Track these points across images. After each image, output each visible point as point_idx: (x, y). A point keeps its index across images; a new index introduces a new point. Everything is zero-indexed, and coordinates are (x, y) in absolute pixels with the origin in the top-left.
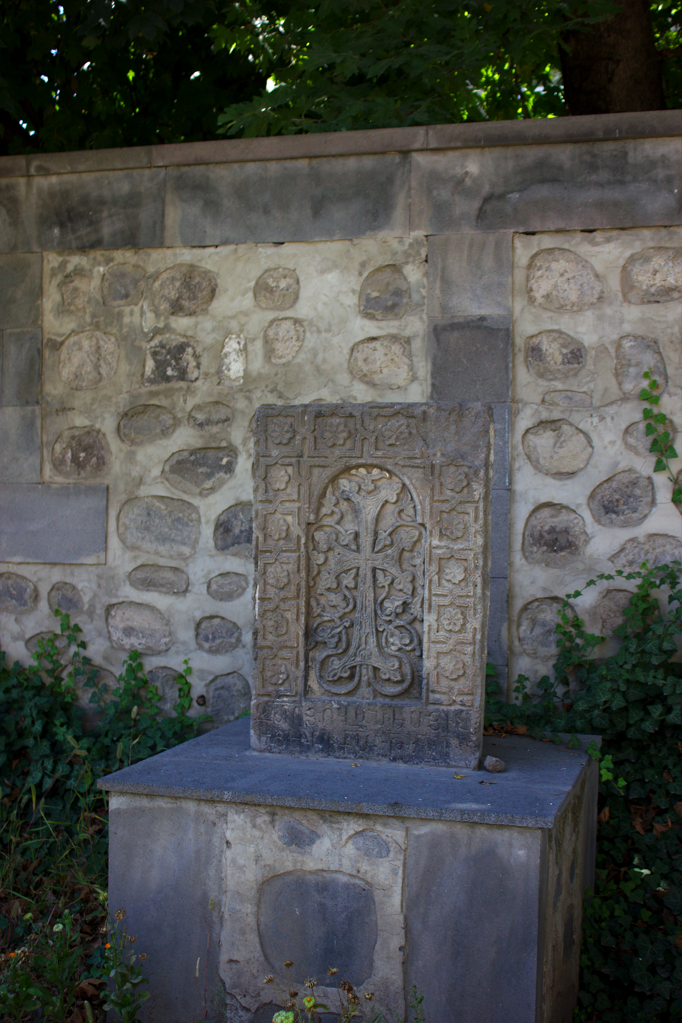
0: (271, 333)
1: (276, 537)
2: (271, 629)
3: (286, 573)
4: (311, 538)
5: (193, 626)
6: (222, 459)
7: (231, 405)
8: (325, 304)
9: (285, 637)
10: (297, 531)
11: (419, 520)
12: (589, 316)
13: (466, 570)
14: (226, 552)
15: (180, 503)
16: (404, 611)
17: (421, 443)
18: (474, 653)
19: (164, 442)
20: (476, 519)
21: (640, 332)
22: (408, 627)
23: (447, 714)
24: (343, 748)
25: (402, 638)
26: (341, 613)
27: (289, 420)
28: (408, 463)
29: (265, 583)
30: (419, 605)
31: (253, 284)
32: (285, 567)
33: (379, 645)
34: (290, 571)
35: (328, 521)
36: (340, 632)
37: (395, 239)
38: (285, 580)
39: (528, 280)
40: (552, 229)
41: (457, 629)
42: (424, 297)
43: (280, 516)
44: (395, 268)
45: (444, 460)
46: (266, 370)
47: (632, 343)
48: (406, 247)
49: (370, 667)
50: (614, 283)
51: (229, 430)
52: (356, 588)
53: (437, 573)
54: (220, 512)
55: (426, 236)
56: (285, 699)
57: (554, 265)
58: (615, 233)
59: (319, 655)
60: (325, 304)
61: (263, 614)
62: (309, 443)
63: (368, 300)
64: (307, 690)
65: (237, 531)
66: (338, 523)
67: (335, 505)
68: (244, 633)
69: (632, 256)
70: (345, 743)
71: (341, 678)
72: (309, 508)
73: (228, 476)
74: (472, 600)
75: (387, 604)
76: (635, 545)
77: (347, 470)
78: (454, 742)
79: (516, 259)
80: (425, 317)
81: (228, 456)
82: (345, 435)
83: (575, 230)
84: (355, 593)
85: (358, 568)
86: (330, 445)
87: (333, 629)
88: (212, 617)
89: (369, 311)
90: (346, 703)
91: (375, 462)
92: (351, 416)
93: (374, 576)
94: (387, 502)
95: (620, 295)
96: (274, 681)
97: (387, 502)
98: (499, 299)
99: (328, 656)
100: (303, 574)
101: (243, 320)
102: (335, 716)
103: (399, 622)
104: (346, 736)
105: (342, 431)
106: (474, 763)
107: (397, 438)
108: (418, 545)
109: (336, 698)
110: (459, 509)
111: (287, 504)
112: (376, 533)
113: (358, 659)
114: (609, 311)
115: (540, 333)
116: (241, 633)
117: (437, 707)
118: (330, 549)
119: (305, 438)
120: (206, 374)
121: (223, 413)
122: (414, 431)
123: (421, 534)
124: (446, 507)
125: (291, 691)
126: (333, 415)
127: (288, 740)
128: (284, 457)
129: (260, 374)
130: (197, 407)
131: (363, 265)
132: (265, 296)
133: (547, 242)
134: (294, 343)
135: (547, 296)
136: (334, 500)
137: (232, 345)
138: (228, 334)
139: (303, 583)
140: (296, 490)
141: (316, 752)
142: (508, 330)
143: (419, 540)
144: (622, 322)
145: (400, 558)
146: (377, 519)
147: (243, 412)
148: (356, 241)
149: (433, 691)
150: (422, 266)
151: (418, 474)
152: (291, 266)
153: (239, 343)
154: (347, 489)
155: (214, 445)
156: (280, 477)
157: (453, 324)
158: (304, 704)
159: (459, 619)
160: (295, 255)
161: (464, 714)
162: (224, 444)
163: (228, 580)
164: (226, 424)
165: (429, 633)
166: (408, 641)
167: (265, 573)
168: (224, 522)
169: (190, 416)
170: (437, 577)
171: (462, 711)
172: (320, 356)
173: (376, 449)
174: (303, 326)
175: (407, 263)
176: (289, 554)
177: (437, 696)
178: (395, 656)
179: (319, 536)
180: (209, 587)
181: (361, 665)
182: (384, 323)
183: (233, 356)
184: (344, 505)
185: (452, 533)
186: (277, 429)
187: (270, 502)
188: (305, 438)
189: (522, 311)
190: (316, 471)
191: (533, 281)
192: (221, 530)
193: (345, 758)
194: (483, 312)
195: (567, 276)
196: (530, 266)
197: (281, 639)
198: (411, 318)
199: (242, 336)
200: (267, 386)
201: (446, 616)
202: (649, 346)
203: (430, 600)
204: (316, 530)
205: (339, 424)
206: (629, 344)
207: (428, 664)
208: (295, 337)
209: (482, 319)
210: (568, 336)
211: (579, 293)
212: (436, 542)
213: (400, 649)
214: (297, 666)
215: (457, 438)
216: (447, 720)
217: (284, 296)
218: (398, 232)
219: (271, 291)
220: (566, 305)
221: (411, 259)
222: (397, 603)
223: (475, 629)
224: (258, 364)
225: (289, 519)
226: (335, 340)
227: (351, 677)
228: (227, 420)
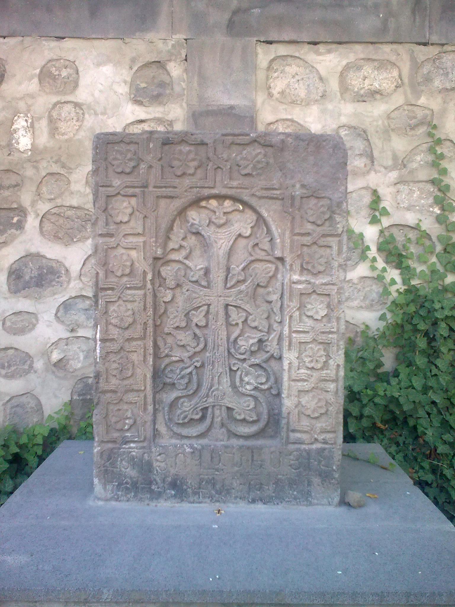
0: (55, 114)
1: (119, 274)
2: (114, 373)
3: (130, 312)
4: (157, 274)
6: (13, 218)
8: (101, 91)
9: (131, 381)
10: (143, 265)
12: (315, 109)
13: (328, 306)
14: (18, 294)
16: (259, 349)
17: (279, 174)
18: (337, 390)
20: (340, 252)
21: (353, 124)
22: (264, 365)
23: (309, 452)
24: (199, 493)
25: (259, 376)
26: (190, 354)
27: (132, 147)
29: (108, 323)
30: (275, 343)
31: (38, 71)
32: (129, 306)
33: (233, 386)
34: (136, 309)
35: (174, 256)
36: (191, 373)
37: (160, 41)
38: (130, 320)
39: (267, 78)
40: (287, 40)
41: (319, 366)
42: (184, 89)
43: (123, 251)
44: (160, 64)
45: (305, 191)
46: (51, 144)
47: (346, 132)
48: (170, 47)
49: (224, 408)
50: (334, 85)
51: (19, 193)
52: (206, 326)
53: (298, 309)
54: (12, 261)
55: (186, 40)
56: (132, 445)
57: (287, 69)
58: (334, 46)
59: (170, 396)
60: (101, 91)
61: (105, 356)
62: (156, 171)
63: (138, 90)
64: (156, 434)
65: (27, 278)
66: (186, 258)
67: (183, 239)
68: (35, 360)
69: (348, 64)
70: (200, 488)
71: (192, 419)
72: (156, 242)
73: (19, 232)
74: (335, 336)
75: (240, 342)
76: (351, 285)
77: (196, 203)
78: (316, 480)
79: (258, 62)
80: (184, 105)
81: (18, 215)
82: (195, 163)
83: (303, 42)
84: (206, 331)
85: (209, 305)
86: (179, 173)
87: (183, 369)
89: (138, 99)
90: (199, 447)
91: (229, 192)
92: (203, 144)
93: (227, 315)
94: (240, 235)
95: (339, 94)
96: (119, 426)
97: (240, 235)
98: (245, 93)
99: (178, 398)
100: (150, 312)
101: (30, 102)
102: (188, 460)
104: (201, 480)
105: (193, 160)
106: (337, 499)
107: (254, 168)
108: (273, 281)
109: (186, 441)
110: (321, 242)
111: (131, 239)
112: (228, 270)
113: (211, 400)
114: (330, 107)
115: (277, 121)
116: (32, 362)
117: (297, 446)
118: (178, 286)
119: (151, 167)
121: (13, 179)
122: (271, 161)
123: (277, 269)
124: (307, 240)
125: (139, 436)
126: (183, 141)
127: (137, 488)
128: (126, 187)
129: (46, 148)
131: (133, 60)
132: (49, 83)
133: (282, 50)
134: (75, 123)
135: (282, 93)
136: (182, 236)
137: (20, 123)
138: (16, 113)
139: (151, 322)
140: (140, 222)
141: (168, 498)
142: (252, 117)
143: (274, 276)
144: (340, 115)
145: (254, 294)
146: (230, 253)
147: (31, 179)
148: (127, 40)
149: (293, 431)
150: (182, 63)
151: (276, 205)
152: (71, 58)
153: (26, 121)
154: (196, 222)
155: (5, 206)
156: (123, 208)
157: (208, 111)
158: (153, 450)
159: (321, 356)
160: (74, 49)
161: (326, 453)
163: (19, 318)
164: (16, 189)
165: (289, 371)
166: (264, 380)
167: (106, 312)
168: (16, 270)
170: (297, 313)
171: (325, 449)
173: (231, 179)
174: (82, 109)
175: (170, 60)
176: (133, 292)
177: (298, 435)
178: (251, 396)
179: (167, 271)
180: (4, 324)
181: (214, 406)
182: (151, 109)
183: (21, 132)
184: (192, 240)
185: (313, 267)
186: (119, 156)
187: (111, 235)
188: (151, 167)
189: (263, 103)
190: (163, 203)
191: (271, 80)
192: (14, 276)
193: (200, 503)
194: (232, 102)
195: (297, 77)
196: (269, 68)
197: (126, 382)
198: (173, 105)
199: (29, 115)
200: (52, 158)
201: (307, 353)
202: (359, 135)
203: (290, 337)
204: (162, 265)
205: (190, 152)
206: (344, 133)
207: (288, 403)
208: (75, 118)
209: (232, 107)
210: (299, 124)
211: (306, 91)
212: (296, 277)
213: (256, 388)
214: (145, 409)
215: (315, 169)
216: (309, 459)
217: (65, 83)
218: (162, 35)
219: (54, 78)
220: (297, 101)
221: (173, 58)
222: (251, 341)
223: (338, 366)
224: (43, 139)
225: (134, 254)
227: (203, 418)
228: (17, 185)
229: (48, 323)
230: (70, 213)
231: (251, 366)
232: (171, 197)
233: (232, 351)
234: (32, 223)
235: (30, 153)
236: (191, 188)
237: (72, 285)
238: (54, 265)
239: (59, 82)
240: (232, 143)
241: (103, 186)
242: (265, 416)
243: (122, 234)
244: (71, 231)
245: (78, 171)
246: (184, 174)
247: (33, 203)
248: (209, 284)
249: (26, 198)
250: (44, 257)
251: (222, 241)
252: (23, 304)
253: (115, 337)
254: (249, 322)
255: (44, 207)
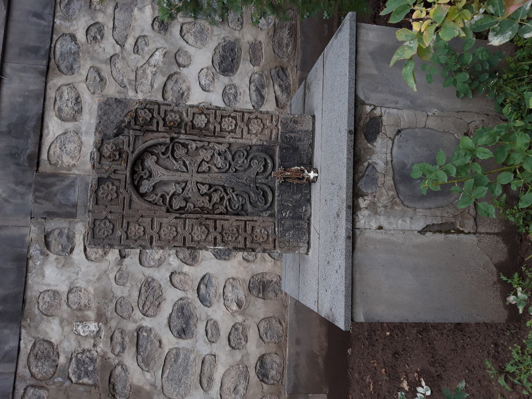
5: (234, 351)
6: (144, 336)
7: (113, 330)
11: (168, 141)
13: (200, 114)
15: (166, 360)
19: (131, 371)
22: (233, 153)
28: (131, 146)
30: (220, 146)
36: (237, 195)
41: (234, 121)
50: (70, 125)
51: (126, 331)
56: (277, 229)
62: (114, 208)
68: (237, 321)
74: (218, 111)
75: (220, 166)
81: (142, 332)
85: (197, 182)
88: (229, 340)
93: (204, 172)
96: (266, 237)
103: (230, 157)
110: (163, 115)
117: (279, 137)
119: (111, 212)
120: (95, 346)
130: (113, 351)
140: (144, 219)
147: (118, 323)
153: (78, 326)
162: (135, 334)
164: (124, 333)
168: (178, 333)
169: (118, 355)
171: (281, 121)
172: (91, 278)
177: (273, 136)
178: (250, 162)
188: (111, 212)
190: (133, 206)
192: (183, 335)
204: (172, 208)
226: (83, 269)
229: (214, 312)
230: (143, 297)
231: (233, 160)
232: (131, 201)
233: (224, 170)
234: (147, 323)
235: (101, 324)
236: (125, 188)
237: (190, 296)
238: (176, 308)
239: (53, 303)
240: (99, 163)
241: (120, 242)
242: (263, 155)
243: (151, 231)
244: (155, 297)
245: (115, 292)
246: (116, 192)
247: (135, 322)
248: (184, 182)
249: (131, 327)
250: (170, 315)
251: (159, 173)
252: (201, 329)
253: (213, 237)
254: (208, 160)
255: (138, 314)
